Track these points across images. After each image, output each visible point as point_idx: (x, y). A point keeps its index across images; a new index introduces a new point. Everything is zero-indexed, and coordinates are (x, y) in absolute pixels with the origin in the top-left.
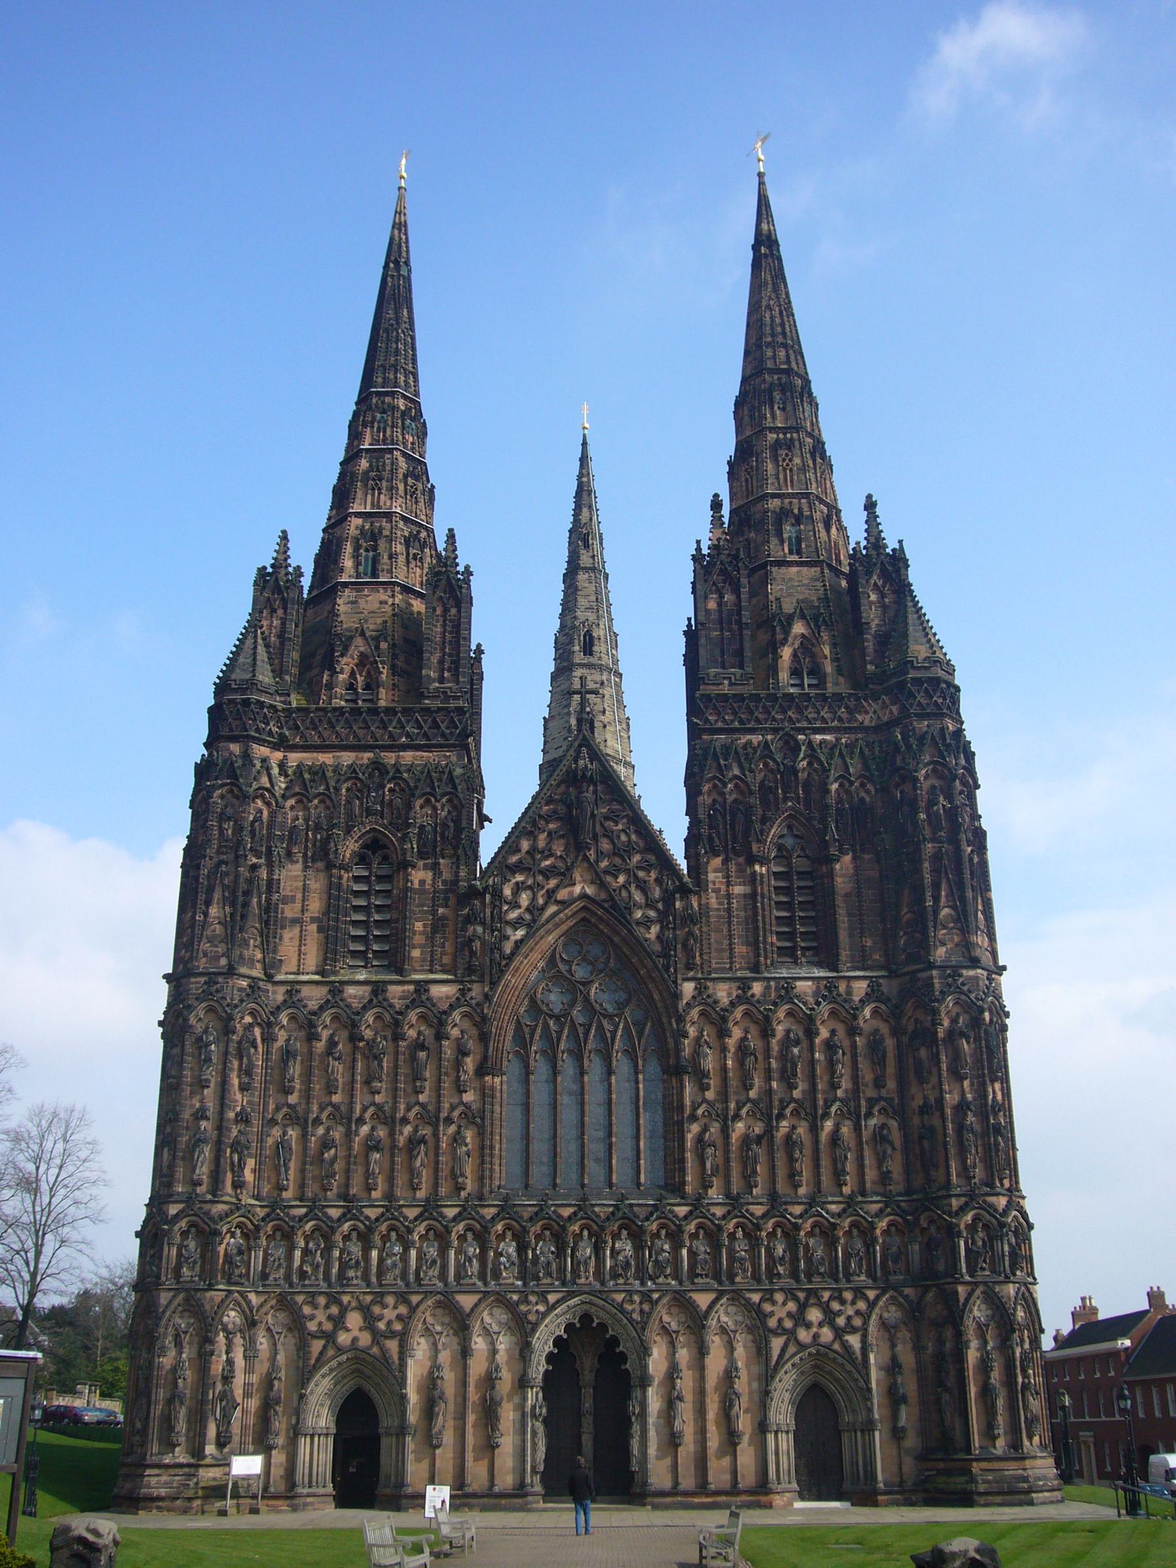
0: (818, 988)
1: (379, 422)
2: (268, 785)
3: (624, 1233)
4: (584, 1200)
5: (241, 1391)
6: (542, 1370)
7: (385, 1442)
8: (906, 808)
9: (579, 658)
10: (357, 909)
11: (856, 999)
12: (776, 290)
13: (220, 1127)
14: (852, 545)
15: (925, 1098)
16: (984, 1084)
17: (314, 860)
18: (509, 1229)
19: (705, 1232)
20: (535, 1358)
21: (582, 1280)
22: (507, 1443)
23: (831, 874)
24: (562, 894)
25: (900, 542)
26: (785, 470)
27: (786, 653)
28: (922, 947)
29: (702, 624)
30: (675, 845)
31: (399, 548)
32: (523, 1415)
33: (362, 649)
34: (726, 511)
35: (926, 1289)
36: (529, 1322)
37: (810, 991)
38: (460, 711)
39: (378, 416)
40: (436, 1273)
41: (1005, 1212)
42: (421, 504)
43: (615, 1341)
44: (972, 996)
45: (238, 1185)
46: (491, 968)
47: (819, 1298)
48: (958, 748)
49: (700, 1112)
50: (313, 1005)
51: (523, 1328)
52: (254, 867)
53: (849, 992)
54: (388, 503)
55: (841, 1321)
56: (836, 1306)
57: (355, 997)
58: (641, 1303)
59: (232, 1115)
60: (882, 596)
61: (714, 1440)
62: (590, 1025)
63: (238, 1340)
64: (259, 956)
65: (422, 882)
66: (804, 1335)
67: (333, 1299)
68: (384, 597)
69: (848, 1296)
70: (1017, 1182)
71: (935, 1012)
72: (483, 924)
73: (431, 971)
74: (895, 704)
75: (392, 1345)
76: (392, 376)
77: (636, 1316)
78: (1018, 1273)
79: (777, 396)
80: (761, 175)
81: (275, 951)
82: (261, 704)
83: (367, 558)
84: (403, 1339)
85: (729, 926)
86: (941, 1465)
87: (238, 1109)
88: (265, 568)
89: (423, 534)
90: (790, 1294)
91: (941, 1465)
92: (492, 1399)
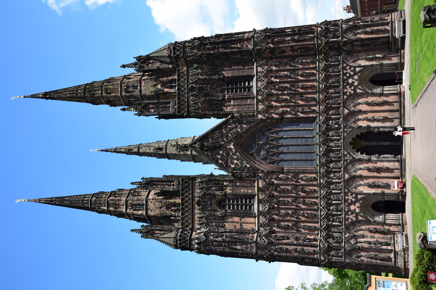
0: (259, 81)
1: (99, 205)
2: (203, 233)
3: (327, 133)
4: (318, 144)
5: (373, 239)
6: (365, 156)
7: (386, 198)
8: (210, 57)
9: (164, 152)
10: (238, 208)
11: (262, 70)
12: (60, 93)
13: (299, 245)
14: (135, 72)
15: (290, 51)
16: (286, 34)
17: (225, 220)
18: (326, 165)
19: (327, 111)
20: (362, 157)
21: (340, 144)
22: (386, 165)
23: (228, 77)
24: (234, 151)
25: (134, 58)
26: (113, 91)
27: (166, 90)
28: (248, 52)
29: (158, 113)
30: (220, 121)
31: (136, 198)
32: (378, 161)
33: (165, 208)
34: (126, 107)
35: (343, 50)
36: (352, 159)
37: (260, 83)
38: (182, 180)
39: (97, 205)
40: (338, 185)
41: (322, 28)
42: (123, 192)
43: (357, 136)
44: (262, 38)
45: (315, 240)
46: (254, 170)
48: (192, 42)
49: (293, 113)
51: (354, 161)
52: (226, 237)
53: (260, 72)
54: (123, 201)
55: (352, 73)
56: (348, 75)
57: (262, 208)
58: (347, 128)
59: (295, 242)
60: (150, 63)
61: (386, 108)
62: (269, 143)
63: (359, 240)
64: (251, 235)
65: (230, 190)
66: (356, 84)
67: (347, 213)
68: (150, 201)
70: (313, 25)
71: (266, 48)
72: (241, 173)
73: (255, 187)
74: (180, 60)
75: (359, 197)
76: (85, 202)
77: (350, 130)
78: (339, 24)
79: (92, 93)
80: (24, 97)
81: (249, 230)
82: (180, 236)
83: (138, 207)
84: (357, 194)
85: (242, 105)
86: (393, 44)
87: (293, 240)
88: (142, 236)
89: (132, 192)
90: (344, 87)
91: (393, 44)
92: (374, 169)
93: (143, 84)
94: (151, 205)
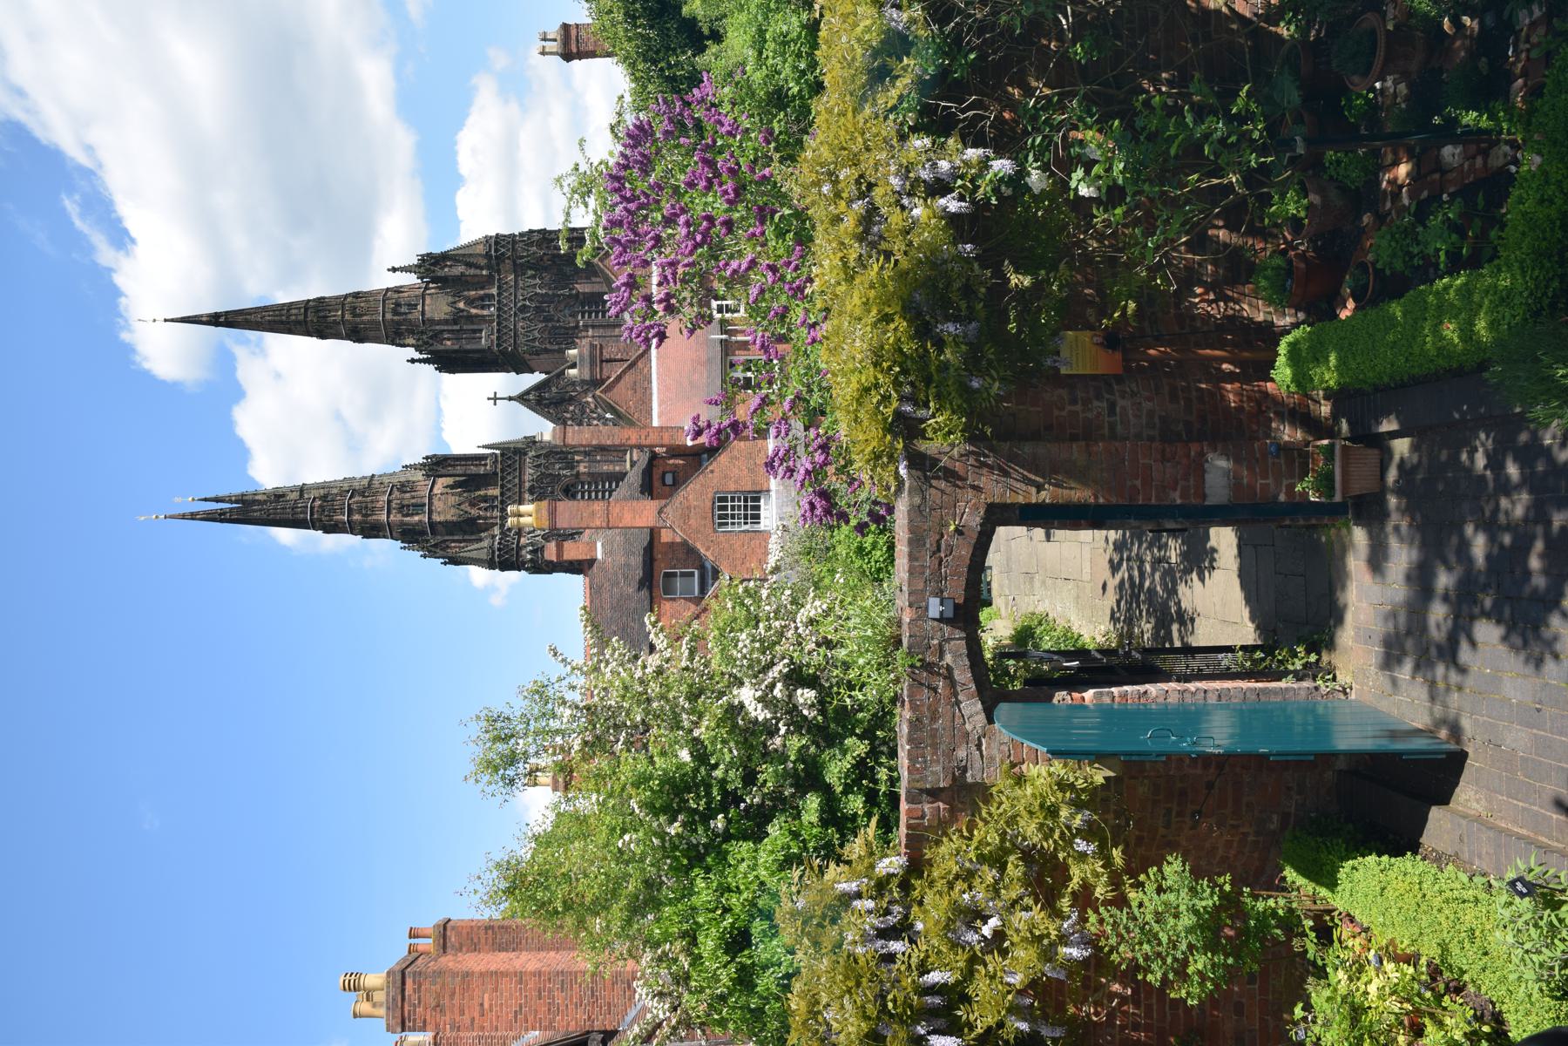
23: (584, 294)
24: (593, 406)
27: (474, 311)
93: (428, 301)
94: (438, 505)
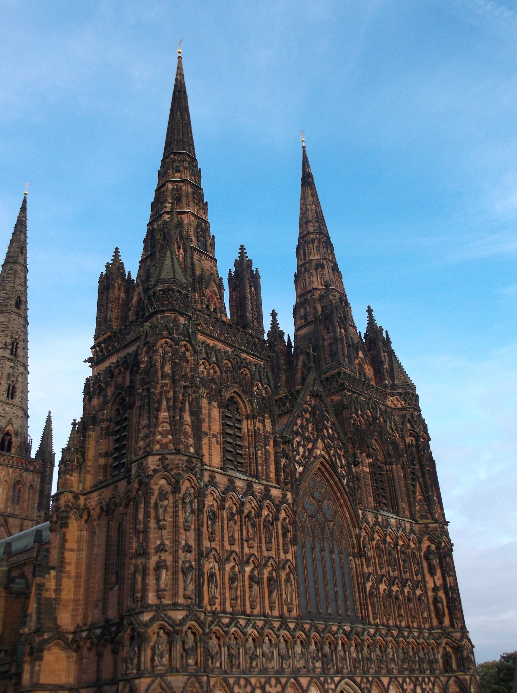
11: (408, 531)
15: (435, 583)
35: (449, 678)
47: (419, 681)
50: (222, 487)
56: (424, 686)
57: (240, 487)
69: (426, 680)
80: (304, 147)
